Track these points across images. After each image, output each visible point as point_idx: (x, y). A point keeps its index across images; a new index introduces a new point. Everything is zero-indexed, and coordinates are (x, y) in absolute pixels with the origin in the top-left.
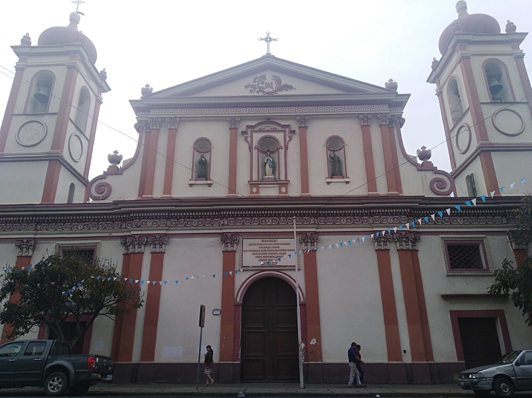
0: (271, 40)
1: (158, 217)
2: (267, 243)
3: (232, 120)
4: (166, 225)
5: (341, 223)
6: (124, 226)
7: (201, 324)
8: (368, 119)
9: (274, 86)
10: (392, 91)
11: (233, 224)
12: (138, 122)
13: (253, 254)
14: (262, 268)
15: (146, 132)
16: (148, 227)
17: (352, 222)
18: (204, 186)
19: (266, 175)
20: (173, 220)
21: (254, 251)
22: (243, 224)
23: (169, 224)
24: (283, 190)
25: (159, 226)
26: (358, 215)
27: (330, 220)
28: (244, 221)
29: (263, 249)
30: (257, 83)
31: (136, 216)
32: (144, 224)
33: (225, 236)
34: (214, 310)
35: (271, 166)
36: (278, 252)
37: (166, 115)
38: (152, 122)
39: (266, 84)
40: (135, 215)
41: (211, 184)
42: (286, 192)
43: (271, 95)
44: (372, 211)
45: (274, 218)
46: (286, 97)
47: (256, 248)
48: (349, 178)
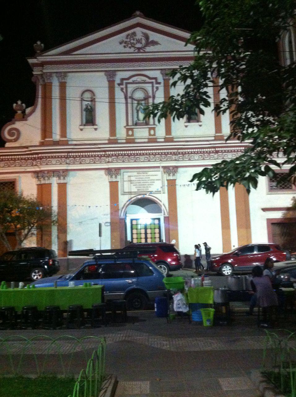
4: (66, 163)
6: (35, 163)
7: (100, 235)
9: (144, 42)
15: (41, 85)
22: (123, 162)
24: (152, 132)
25: (61, 164)
26: (207, 152)
29: (138, 179)
32: (50, 162)
33: (110, 170)
34: (106, 223)
36: (149, 181)
39: (137, 40)
42: (154, 135)
43: (141, 51)
45: (145, 156)
48: (201, 122)
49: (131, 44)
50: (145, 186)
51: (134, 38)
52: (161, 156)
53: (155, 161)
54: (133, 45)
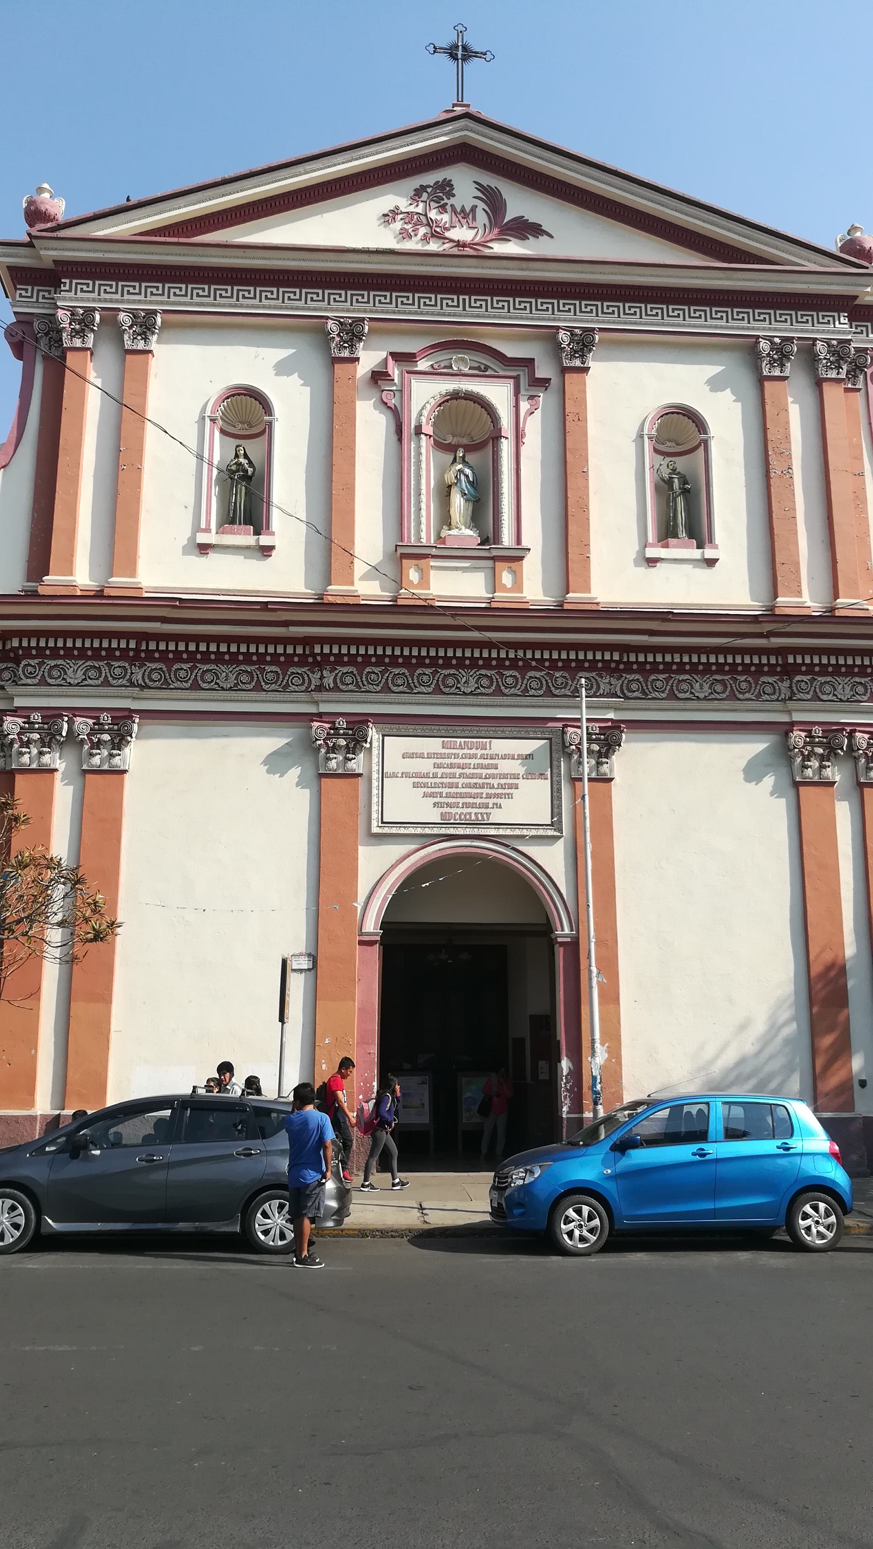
0: (468, 54)
1: (103, 653)
2: (461, 752)
3: (341, 331)
4: (130, 680)
5: (692, 693)
7: (282, 1019)
8: (785, 356)
9: (482, 218)
10: (867, 268)
11: (351, 687)
12: (18, 321)
13: (415, 785)
14: (443, 831)
15: (46, 358)
16: (70, 685)
17: (727, 693)
18: (246, 552)
19: (450, 524)
20: (154, 666)
21: (418, 775)
22: (387, 689)
23: (140, 677)
24: (506, 578)
25: (106, 683)
27: (659, 684)
28: (387, 680)
29: (448, 771)
30: (421, 205)
31: (29, 648)
32: (55, 673)
35: (469, 497)
36: (495, 782)
37: (117, 301)
38: (70, 324)
40: (25, 644)
41: (272, 548)
42: (518, 585)
44: (791, 660)
45: (483, 672)
46: (524, 264)
47: (426, 766)
49: (429, 223)
50: (478, 801)
51: (442, 202)
52: (551, 676)
53: (525, 693)
54: (438, 230)
